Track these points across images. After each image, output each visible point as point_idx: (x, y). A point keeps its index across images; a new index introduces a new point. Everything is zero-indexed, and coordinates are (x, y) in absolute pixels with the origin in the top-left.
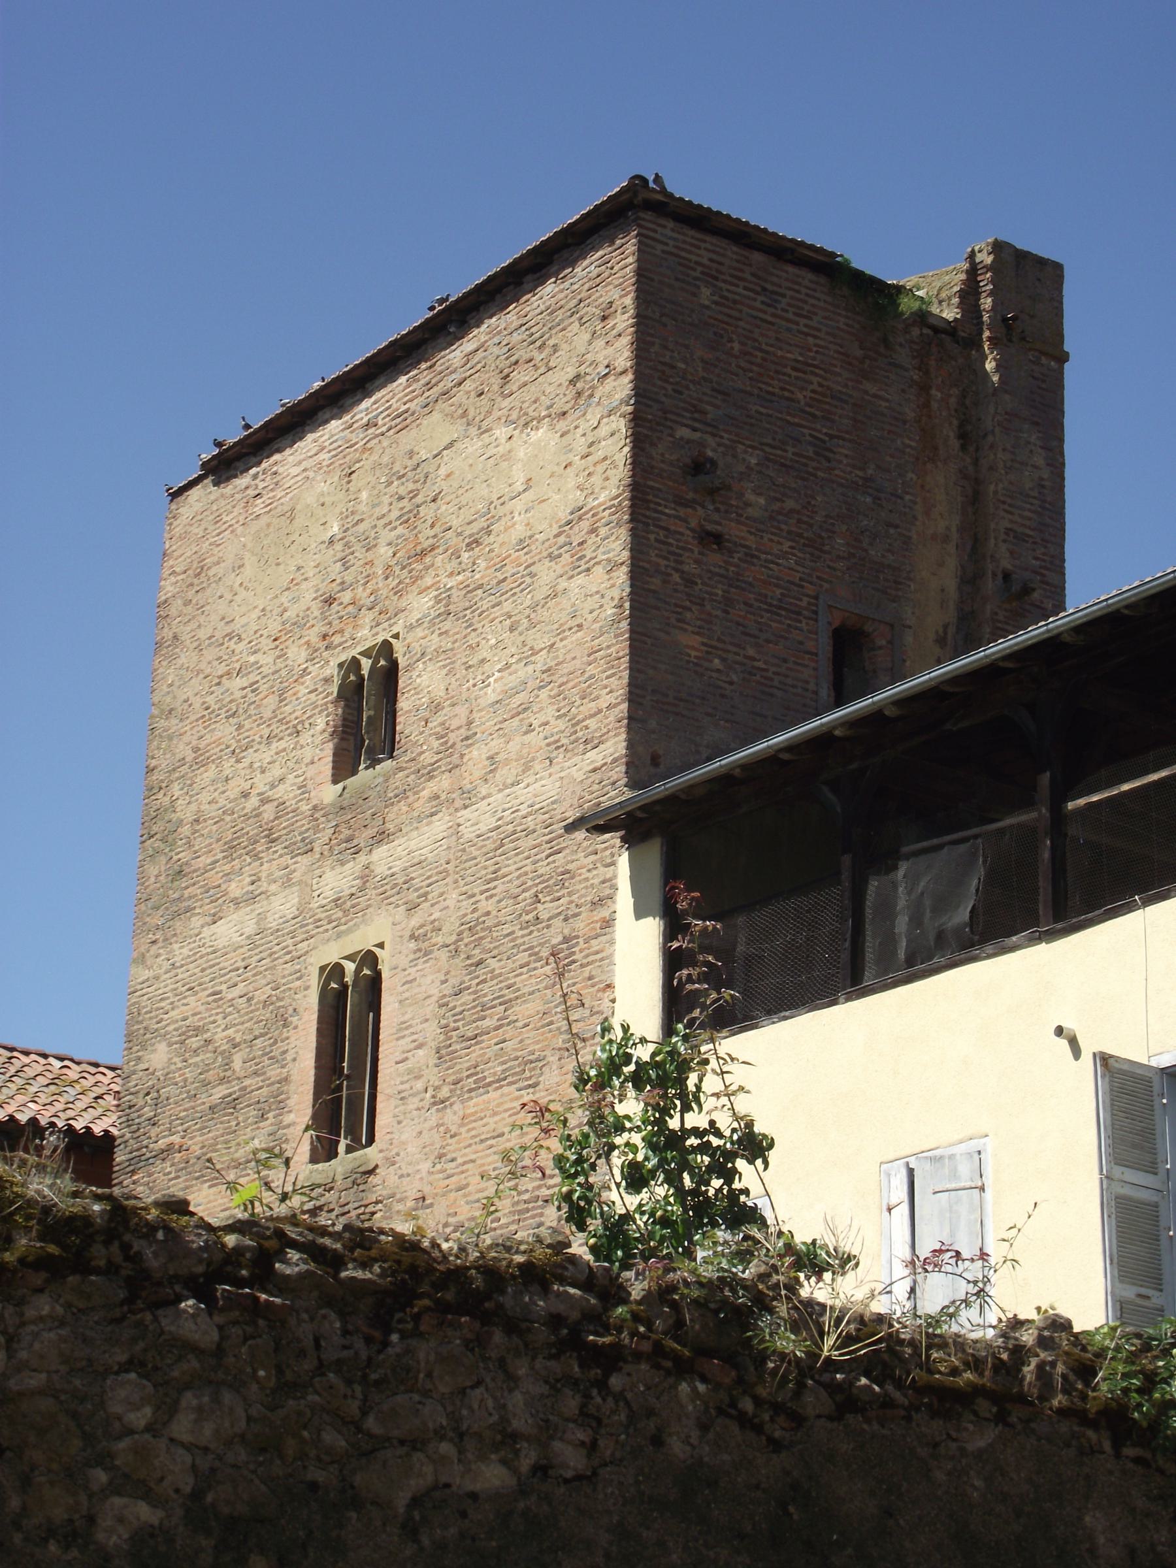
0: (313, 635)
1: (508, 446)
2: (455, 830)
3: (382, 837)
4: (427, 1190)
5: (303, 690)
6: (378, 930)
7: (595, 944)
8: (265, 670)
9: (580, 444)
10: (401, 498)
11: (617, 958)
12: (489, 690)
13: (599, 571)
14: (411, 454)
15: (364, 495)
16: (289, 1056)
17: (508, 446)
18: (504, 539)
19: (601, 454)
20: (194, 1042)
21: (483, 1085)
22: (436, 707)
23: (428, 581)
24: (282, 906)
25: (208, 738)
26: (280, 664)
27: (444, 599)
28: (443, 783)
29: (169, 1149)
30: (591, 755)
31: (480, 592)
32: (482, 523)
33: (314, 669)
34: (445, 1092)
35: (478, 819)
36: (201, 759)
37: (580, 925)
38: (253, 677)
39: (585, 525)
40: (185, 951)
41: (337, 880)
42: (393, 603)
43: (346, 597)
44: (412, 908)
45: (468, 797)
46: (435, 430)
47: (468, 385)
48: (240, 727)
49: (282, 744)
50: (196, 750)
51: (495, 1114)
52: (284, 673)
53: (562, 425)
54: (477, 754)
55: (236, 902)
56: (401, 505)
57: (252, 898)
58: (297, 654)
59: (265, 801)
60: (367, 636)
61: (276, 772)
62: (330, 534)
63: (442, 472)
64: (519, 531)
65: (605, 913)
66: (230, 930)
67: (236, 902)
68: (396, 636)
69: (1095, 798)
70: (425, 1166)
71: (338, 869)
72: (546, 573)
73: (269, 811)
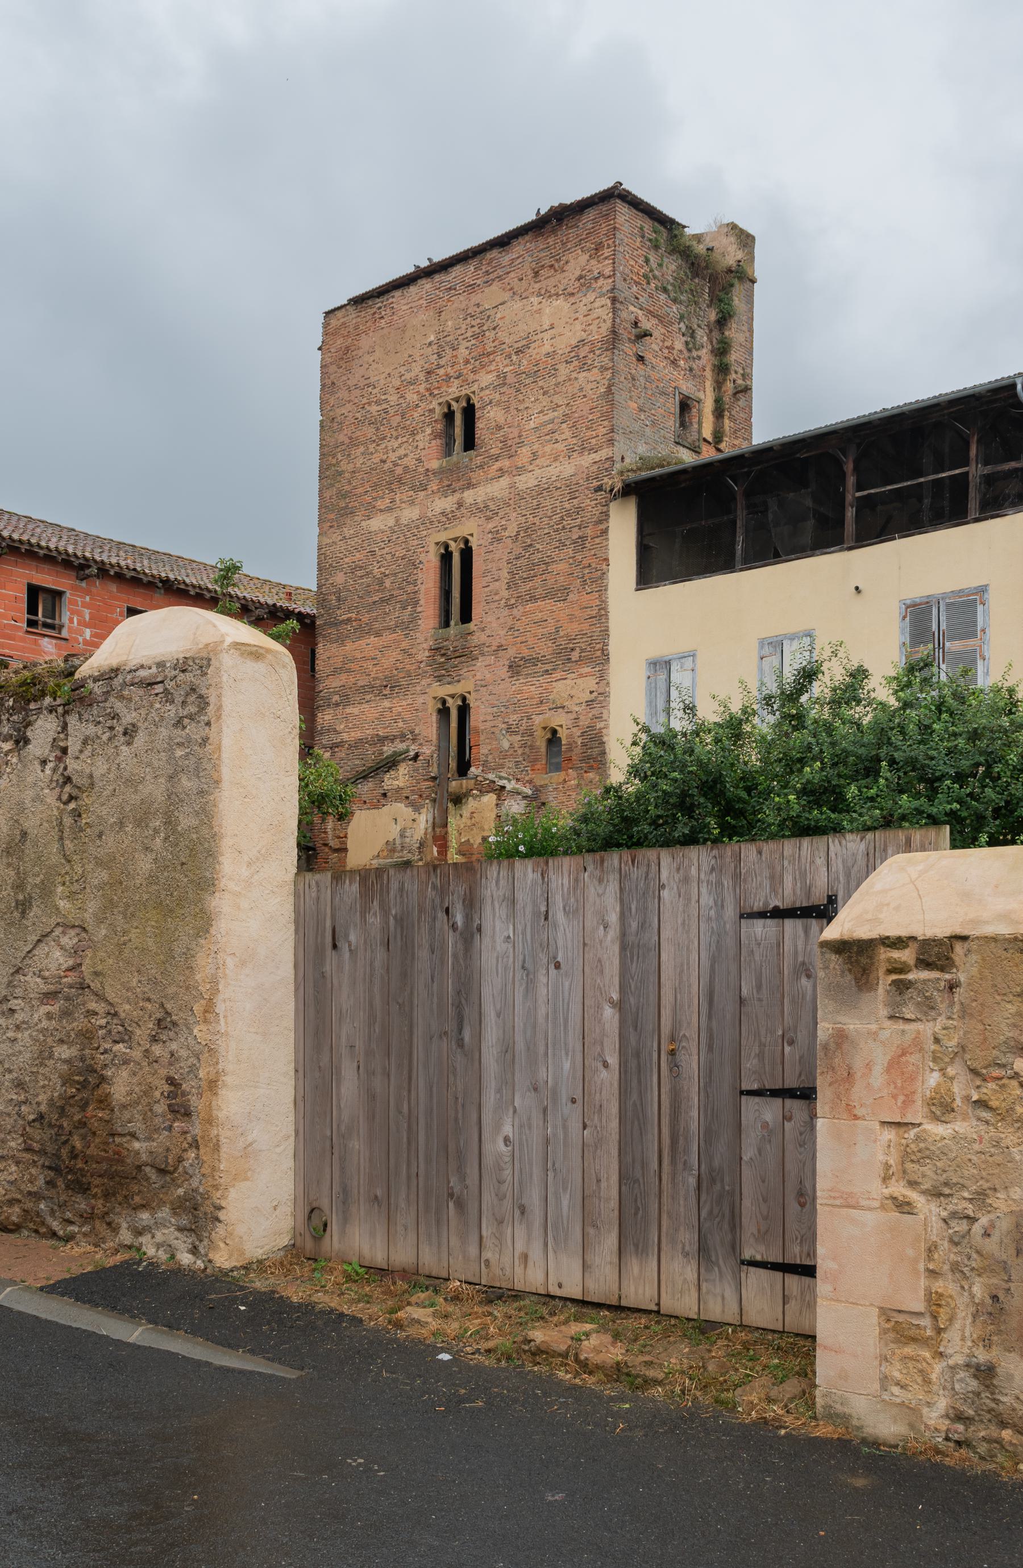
0: (422, 388)
1: (539, 307)
3: (470, 486)
4: (504, 642)
5: (416, 415)
6: (469, 527)
7: (597, 540)
8: (392, 403)
9: (583, 310)
10: (473, 326)
11: (610, 547)
12: (531, 422)
13: (595, 370)
14: (478, 305)
15: (450, 323)
16: (419, 582)
17: (539, 307)
18: (540, 350)
19: (595, 315)
20: (359, 573)
21: (533, 599)
22: (499, 428)
24: (409, 514)
25: (359, 433)
26: (401, 401)
27: (502, 377)
28: (505, 463)
29: (349, 620)
30: (593, 455)
31: (524, 375)
32: (524, 342)
33: (423, 405)
34: (513, 601)
35: (526, 481)
36: (353, 442)
37: (589, 532)
38: (384, 406)
39: (587, 348)
40: (352, 532)
41: (447, 503)
42: (471, 377)
43: (441, 372)
44: (489, 519)
45: (520, 470)
46: (491, 295)
47: (512, 275)
48: (378, 429)
49: (405, 439)
50: (350, 438)
51: (541, 612)
52: (404, 405)
53: (572, 300)
54: (525, 452)
55: (381, 511)
56: (473, 329)
57: (389, 509)
58: (412, 397)
59: (396, 465)
60: (454, 390)
61: (401, 452)
62: (429, 340)
63: (499, 316)
64: (547, 348)
65: (603, 527)
66: (378, 523)
67: (381, 511)
68: (474, 393)
69: (872, 491)
70: (503, 633)
71: (443, 499)
72: (563, 370)
73: (399, 470)
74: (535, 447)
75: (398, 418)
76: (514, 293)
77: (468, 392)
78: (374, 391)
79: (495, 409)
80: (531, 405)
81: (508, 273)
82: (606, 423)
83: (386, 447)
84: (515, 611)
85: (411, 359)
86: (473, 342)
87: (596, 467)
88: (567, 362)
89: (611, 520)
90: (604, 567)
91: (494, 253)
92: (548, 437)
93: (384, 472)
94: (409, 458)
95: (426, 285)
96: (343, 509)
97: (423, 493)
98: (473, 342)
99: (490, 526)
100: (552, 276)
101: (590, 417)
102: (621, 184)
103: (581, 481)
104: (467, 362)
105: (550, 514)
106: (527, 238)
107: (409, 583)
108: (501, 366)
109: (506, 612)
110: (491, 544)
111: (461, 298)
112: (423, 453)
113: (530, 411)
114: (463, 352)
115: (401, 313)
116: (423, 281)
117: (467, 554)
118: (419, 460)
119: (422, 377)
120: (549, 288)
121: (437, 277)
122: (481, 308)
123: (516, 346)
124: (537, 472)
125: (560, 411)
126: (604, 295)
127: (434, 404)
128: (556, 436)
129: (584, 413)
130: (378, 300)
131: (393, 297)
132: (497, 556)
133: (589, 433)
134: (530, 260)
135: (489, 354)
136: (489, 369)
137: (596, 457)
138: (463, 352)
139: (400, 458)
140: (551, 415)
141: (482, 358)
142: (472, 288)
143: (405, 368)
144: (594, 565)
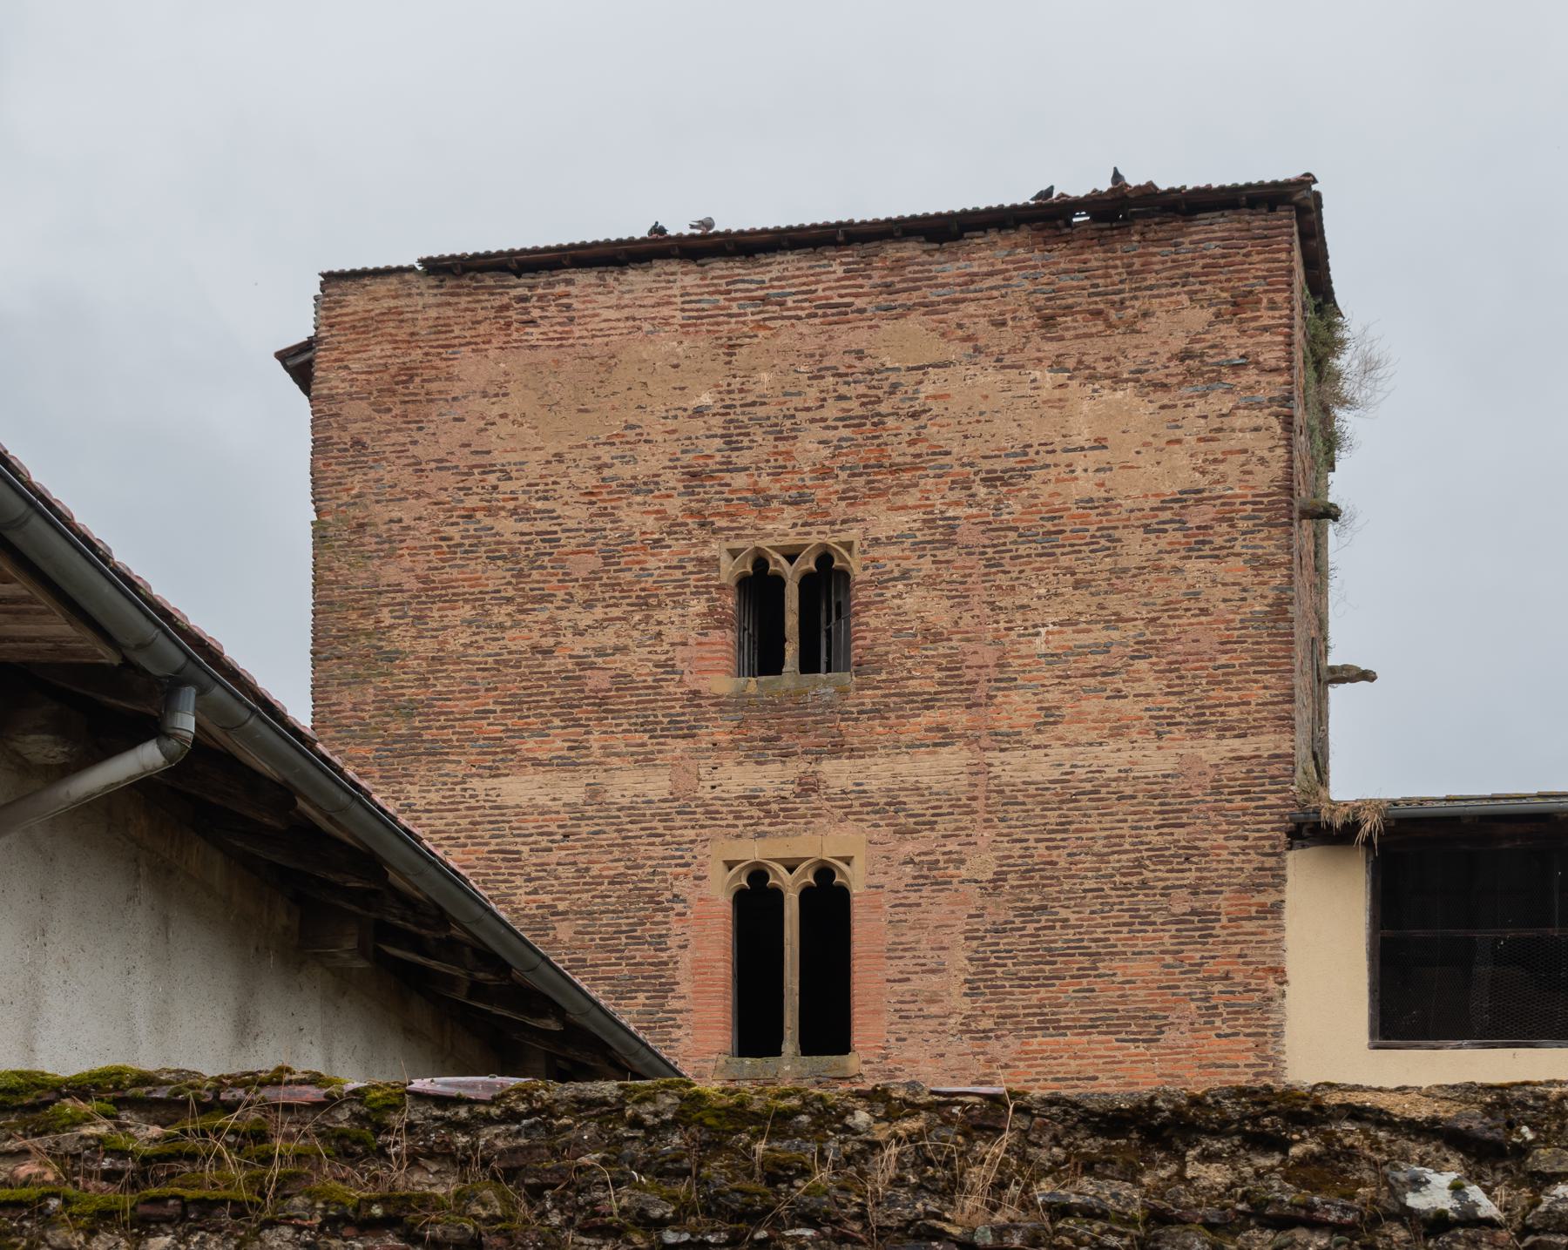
0: (674, 507)
8: (571, 524)
12: (1038, 640)
17: (1058, 393)
19: (1234, 444)
21: (1051, 1025)
23: (912, 498)
30: (1237, 743)
31: (1012, 535)
34: (987, 1023)
36: (433, 591)
38: (543, 525)
40: (434, 797)
43: (740, 480)
44: (903, 832)
45: (1007, 740)
46: (901, 342)
49: (616, 612)
50: (425, 580)
51: (1076, 1057)
55: (537, 763)
56: (844, 404)
61: (607, 638)
62: (695, 403)
63: (928, 389)
64: (1085, 486)
65: (1268, 898)
67: (537, 763)
68: (848, 546)
71: (750, 766)
72: (1136, 548)
74: (1053, 697)
75: (595, 562)
76: (977, 349)
77: (831, 541)
78: (506, 486)
79: (920, 592)
80: (1035, 603)
81: (956, 302)
82: (1271, 680)
83: (552, 620)
84: (994, 1047)
85: (632, 437)
86: (846, 433)
87: (1239, 769)
88: (1147, 529)
89: (1288, 887)
92: (1091, 682)
93: (547, 676)
94: (633, 657)
95: (687, 279)
96: (399, 738)
98: (846, 433)
99: (909, 847)
100: (1098, 334)
101: (1223, 659)
102: (1315, 181)
103: (1198, 793)
104: (824, 473)
105: (1099, 847)
107: (639, 940)
108: (935, 499)
109: (966, 1044)
110: (914, 887)
111: (802, 328)
112: (680, 653)
113: (1034, 617)
114: (810, 448)
115: (594, 324)
118: (668, 666)
119: (672, 479)
120: (1088, 360)
121: (719, 269)
122: (868, 363)
123: (986, 465)
124: (1059, 752)
125: (1131, 631)
126: (1260, 406)
127: (716, 548)
128: (1117, 682)
129: (1204, 646)
131: (569, 282)
132: (934, 917)
133: (1218, 693)
134: (1028, 285)
135: (896, 469)
136: (899, 501)
137: (1246, 747)
138: (810, 448)
139: (601, 652)
140: (1099, 635)
141: (878, 475)
142: (839, 313)
143: (615, 451)
144: (1238, 978)
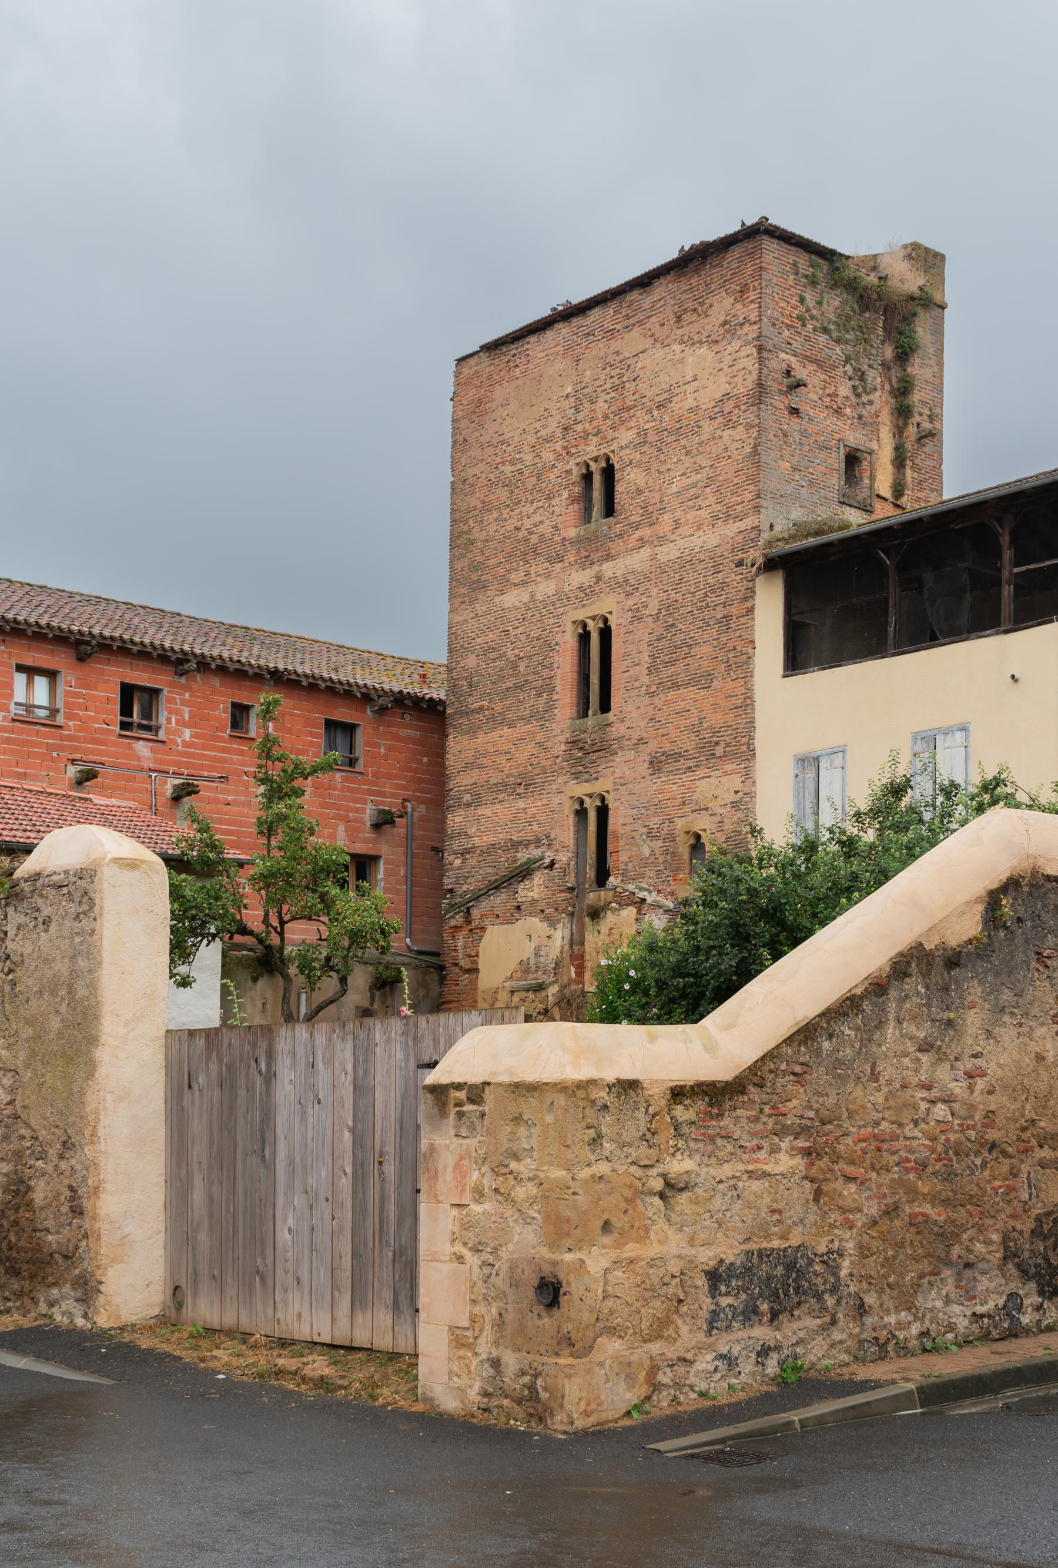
0: (558, 447)
1: (681, 356)
2: (653, 558)
3: (609, 557)
4: (644, 735)
5: (552, 476)
6: (608, 604)
7: (743, 620)
9: (727, 360)
10: (612, 377)
11: (756, 628)
12: (674, 485)
13: (741, 428)
14: (618, 353)
15: (588, 373)
16: (555, 666)
17: (681, 356)
18: (682, 404)
19: (741, 366)
20: (492, 656)
21: (676, 686)
22: (640, 492)
23: (632, 424)
24: (546, 589)
25: (492, 497)
26: (537, 460)
27: (643, 434)
28: (646, 532)
29: (481, 708)
30: (738, 524)
31: (666, 433)
32: (666, 396)
33: (559, 465)
34: (654, 688)
35: (668, 553)
37: (734, 610)
38: (519, 466)
39: (731, 403)
40: (484, 608)
41: (582, 577)
42: (610, 434)
43: (579, 428)
44: (628, 595)
45: (662, 540)
46: (632, 342)
47: (653, 319)
48: (512, 492)
49: (540, 504)
50: (483, 502)
52: (539, 465)
53: (716, 348)
54: (667, 519)
55: (515, 585)
56: (612, 380)
57: (524, 583)
58: (548, 456)
59: (531, 533)
60: (592, 449)
61: (537, 518)
62: (566, 392)
63: (639, 365)
64: (690, 403)
65: (748, 604)
66: (513, 599)
67: (515, 585)
68: (613, 452)
70: (643, 724)
71: (581, 572)
72: (707, 428)
73: (534, 539)
75: (534, 480)
76: (655, 340)
77: (607, 451)
80: (673, 467)
81: (649, 317)
82: (751, 488)
83: (521, 512)
84: (656, 700)
86: (613, 394)
89: (757, 597)
90: (750, 650)
91: (634, 295)
92: (691, 503)
94: (545, 525)
95: (563, 330)
96: (475, 582)
97: (559, 565)
98: (613, 394)
99: (630, 603)
100: (695, 321)
102: (767, 219)
103: (726, 553)
106: (669, 278)
109: (647, 700)
110: (631, 623)
111: (600, 345)
113: (672, 474)
114: (602, 406)
116: (560, 325)
117: (606, 634)
119: (559, 433)
121: (575, 321)
122: (621, 357)
123: (658, 399)
124: (680, 542)
125: (705, 473)
127: (571, 465)
128: (700, 501)
129: (729, 476)
130: (512, 346)
131: (528, 343)
133: (735, 498)
135: (629, 409)
137: (741, 525)
138: (602, 406)
140: (695, 478)
141: (622, 412)
142: (611, 334)
143: (541, 423)
144: (739, 648)
